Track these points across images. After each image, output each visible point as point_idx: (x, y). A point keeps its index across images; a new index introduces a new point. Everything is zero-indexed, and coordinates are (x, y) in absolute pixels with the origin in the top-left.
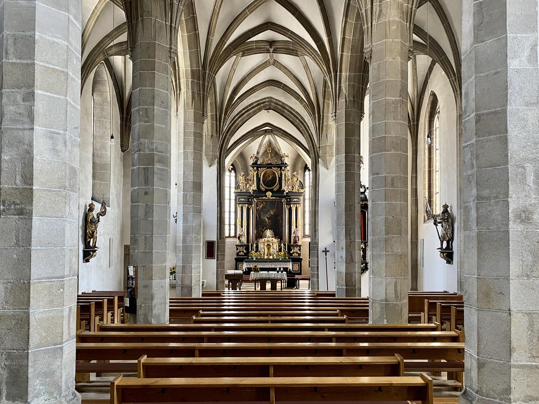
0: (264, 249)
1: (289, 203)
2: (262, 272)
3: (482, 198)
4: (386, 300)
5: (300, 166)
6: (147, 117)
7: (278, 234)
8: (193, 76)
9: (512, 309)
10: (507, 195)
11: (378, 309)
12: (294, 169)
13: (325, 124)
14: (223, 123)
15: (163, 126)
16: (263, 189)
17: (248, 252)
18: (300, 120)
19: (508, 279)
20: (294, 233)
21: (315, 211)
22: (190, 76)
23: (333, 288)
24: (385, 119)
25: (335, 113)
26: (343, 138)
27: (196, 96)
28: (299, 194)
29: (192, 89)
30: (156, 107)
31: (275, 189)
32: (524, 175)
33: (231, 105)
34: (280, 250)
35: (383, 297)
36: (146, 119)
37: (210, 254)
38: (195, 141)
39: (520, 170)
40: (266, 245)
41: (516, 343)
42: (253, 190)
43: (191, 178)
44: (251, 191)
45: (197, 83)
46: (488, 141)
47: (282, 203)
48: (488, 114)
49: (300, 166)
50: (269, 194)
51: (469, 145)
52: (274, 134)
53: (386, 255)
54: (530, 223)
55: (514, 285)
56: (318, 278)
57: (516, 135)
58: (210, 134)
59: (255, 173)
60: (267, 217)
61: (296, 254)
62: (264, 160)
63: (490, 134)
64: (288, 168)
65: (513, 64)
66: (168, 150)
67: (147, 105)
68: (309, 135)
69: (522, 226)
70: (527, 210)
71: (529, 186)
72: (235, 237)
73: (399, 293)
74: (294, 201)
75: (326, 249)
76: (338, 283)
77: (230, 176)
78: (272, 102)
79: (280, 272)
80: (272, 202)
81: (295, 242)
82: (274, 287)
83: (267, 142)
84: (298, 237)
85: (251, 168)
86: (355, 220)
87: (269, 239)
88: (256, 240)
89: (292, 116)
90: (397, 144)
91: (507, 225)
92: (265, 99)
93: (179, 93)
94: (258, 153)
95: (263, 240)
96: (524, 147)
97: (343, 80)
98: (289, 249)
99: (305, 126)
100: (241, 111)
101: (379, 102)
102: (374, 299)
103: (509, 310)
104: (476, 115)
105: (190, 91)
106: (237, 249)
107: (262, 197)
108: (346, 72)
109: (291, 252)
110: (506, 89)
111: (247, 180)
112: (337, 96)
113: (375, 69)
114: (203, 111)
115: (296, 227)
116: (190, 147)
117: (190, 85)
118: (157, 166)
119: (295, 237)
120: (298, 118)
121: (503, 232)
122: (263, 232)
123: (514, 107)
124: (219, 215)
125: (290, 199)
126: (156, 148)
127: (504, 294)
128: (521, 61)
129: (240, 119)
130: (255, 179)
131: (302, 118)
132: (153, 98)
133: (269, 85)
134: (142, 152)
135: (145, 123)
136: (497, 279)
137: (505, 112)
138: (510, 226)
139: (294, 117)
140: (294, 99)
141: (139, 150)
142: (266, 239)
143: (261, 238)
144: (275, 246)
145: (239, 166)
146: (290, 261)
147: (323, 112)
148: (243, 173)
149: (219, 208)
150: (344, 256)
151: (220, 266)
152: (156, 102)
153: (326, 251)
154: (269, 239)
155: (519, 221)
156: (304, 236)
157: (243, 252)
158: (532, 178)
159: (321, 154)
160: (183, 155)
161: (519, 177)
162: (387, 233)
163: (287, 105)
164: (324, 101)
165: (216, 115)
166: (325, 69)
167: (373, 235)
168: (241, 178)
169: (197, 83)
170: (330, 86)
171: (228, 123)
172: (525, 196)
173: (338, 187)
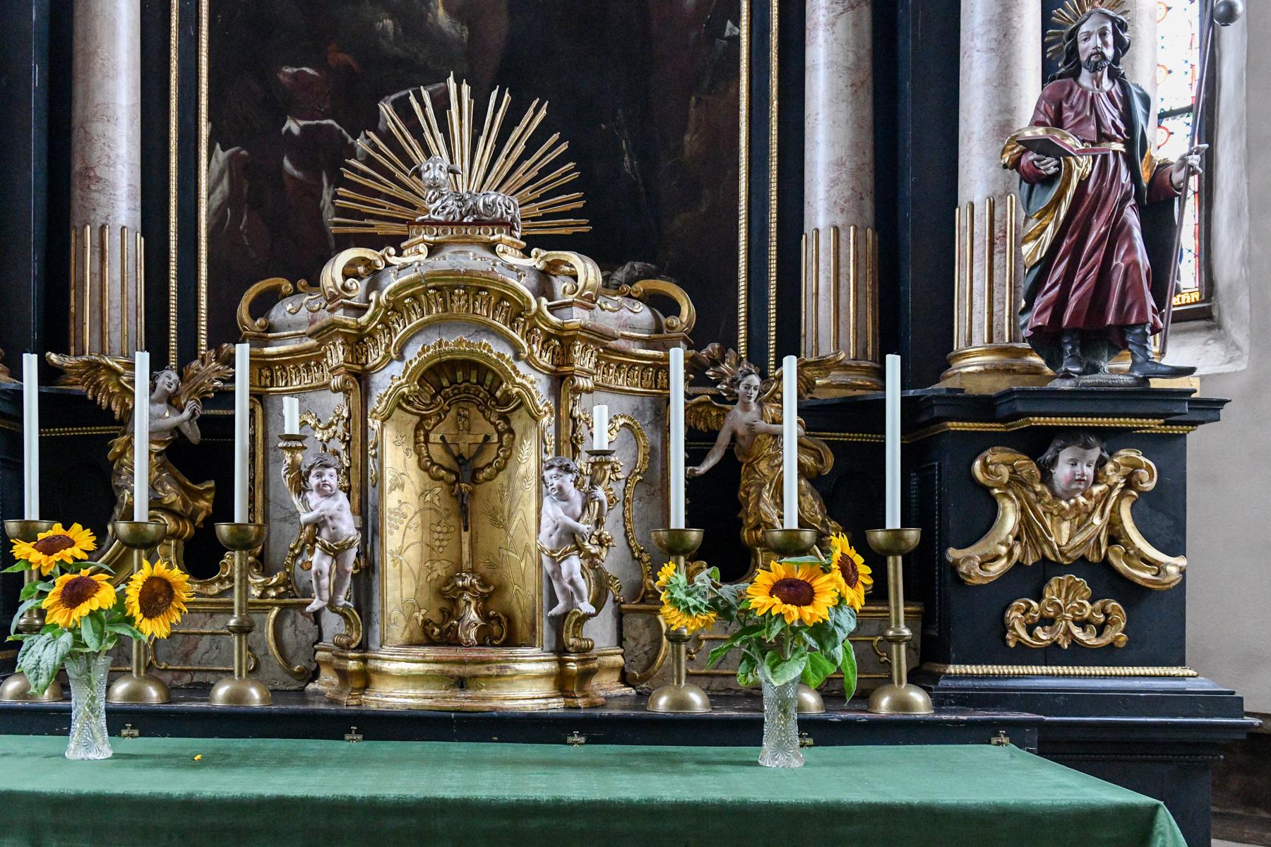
0: (365, 495)
40: (389, 379)
109: (984, 560)
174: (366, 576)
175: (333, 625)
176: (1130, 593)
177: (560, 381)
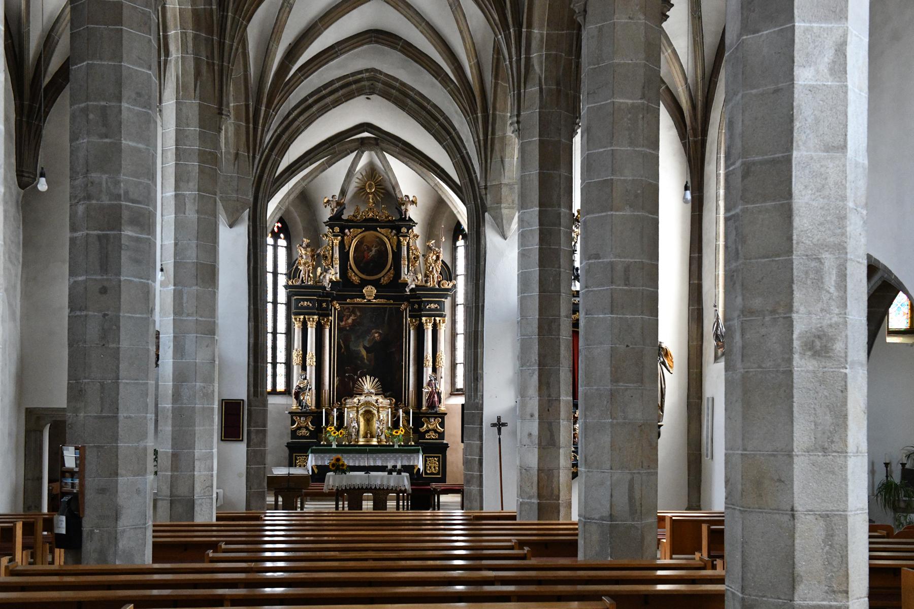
1: (417, 314)
2: (352, 473)
3: (752, 313)
4: (611, 517)
5: (443, 225)
6: (105, 125)
7: (391, 387)
8: (197, 25)
9: (798, 507)
10: (790, 308)
11: (595, 537)
12: (430, 232)
13: (498, 134)
14: (263, 126)
15: (141, 146)
16: (355, 279)
17: (318, 431)
18: (441, 125)
19: (790, 455)
20: (429, 384)
21: (476, 332)
22: (190, 25)
23: (511, 507)
24: (611, 144)
25: (518, 115)
26: (534, 172)
27: (204, 69)
28: (442, 293)
29: (196, 53)
30: (125, 105)
31: (384, 281)
32: (819, 272)
33: (284, 83)
34: (396, 425)
35: (605, 512)
36: (104, 130)
37: (231, 432)
38: (201, 171)
39: (813, 264)
40: (361, 412)
41: (804, 568)
42: (331, 281)
43: (192, 255)
44: (326, 283)
45: (206, 39)
46: (760, 211)
47: (399, 314)
48: (762, 163)
49: (443, 225)
50: (370, 291)
51: (733, 216)
52: (382, 150)
53: (612, 425)
54: (830, 357)
55: (801, 466)
56: (481, 485)
57: (807, 203)
58: (233, 151)
59: (336, 242)
60: (365, 348)
61: (432, 435)
62: (357, 210)
63: (765, 198)
64: (416, 230)
65: (804, 76)
66: (149, 197)
67: (104, 99)
68: (463, 157)
69: (815, 362)
70: (825, 335)
71: (828, 292)
72: (287, 392)
73: (638, 504)
74: (430, 310)
75: (499, 419)
76: (522, 492)
77: (275, 247)
78: (378, 80)
79: (394, 474)
80: (377, 311)
81: (432, 405)
82: (380, 504)
83: (364, 168)
84: (439, 394)
85: (327, 229)
86: (559, 354)
87: (369, 399)
88: (339, 399)
89: (424, 113)
90: (636, 196)
91: (790, 360)
92: (360, 72)
93: (166, 62)
94: (343, 192)
95: (356, 400)
96: (821, 224)
97: (535, 44)
98: (418, 423)
99: (452, 139)
100: (305, 100)
101: (600, 108)
102: (587, 516)
103: (792, 510)
104: (743, 164)
105: (190, 57)
106: (293, 423)
107: (352, 297)
108: (541, 28)
110: (791, 120)
111: (317, 258)
112: (523, 77)
113: (593, 37)
114: (221, 104)
115: (435, 370)
116: (191, 184)
117: (190, 44)
118: (128, 232)
119: (431, 394)
120: (437, 120)
121: (784, 372)
122: (355, 382)
123: (805, 153)
124: (252, 341)
125: (419, 304)
126: (126, 193)
127: (784, 482)
128: (817, 72)
129: (302, 118)
130: (337, 255)
131: (447, 119)
132: (119, 83)
133: (370, 42)
134: (94, 202)
135: (102, 138)
136: (774, 455)
137: (788, 160)
138: (795, 363)
139: (429, 117)
140: (428, 77)
141: (89, 197)
142: (362, 398)
143: (352, 396)
144: (383, 415)
145: (298, 223)
146: (417, 452)
147: (494, 109)
148: (306, 241)
149: (252, 324)
150: (535, 432)
151: (255, 458)
152: (126, 93)
153: (499, 425)
154: (369, 399)
155: (809, 353)
156: (454, 392)
157: (307, 428)
158: (834, 277)
159: (489, 202)
160: (173, 202)
161: (812, 276)
162: (615, 380)
163: (413, 89)
164: (496, 85)
165: (247, 106)
166: (496, 17)
167: (588, 384)
168: (303, 253)
169: (206, 39)
170: (507, 56)
171: (274, 126)
172: (822, 310)
173: (523, 280)
174: (358, 431)
175: (354, 437)
176: (439, 433)
177: (378, 412)
